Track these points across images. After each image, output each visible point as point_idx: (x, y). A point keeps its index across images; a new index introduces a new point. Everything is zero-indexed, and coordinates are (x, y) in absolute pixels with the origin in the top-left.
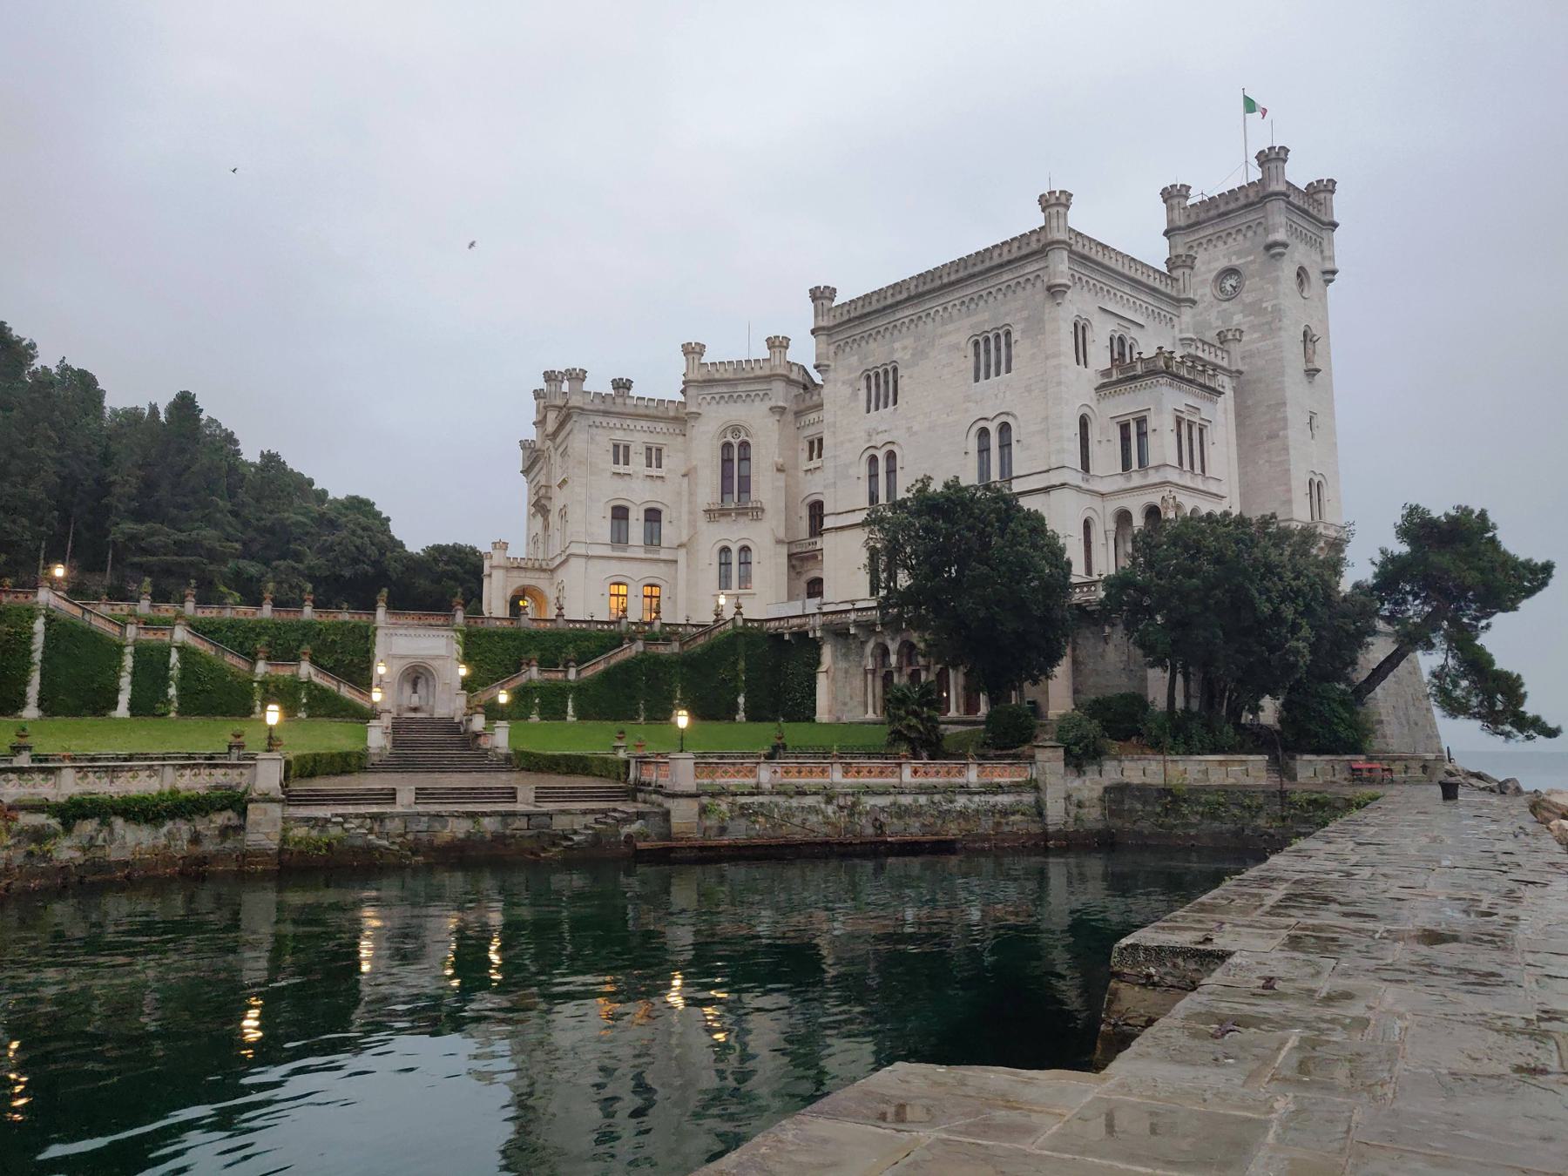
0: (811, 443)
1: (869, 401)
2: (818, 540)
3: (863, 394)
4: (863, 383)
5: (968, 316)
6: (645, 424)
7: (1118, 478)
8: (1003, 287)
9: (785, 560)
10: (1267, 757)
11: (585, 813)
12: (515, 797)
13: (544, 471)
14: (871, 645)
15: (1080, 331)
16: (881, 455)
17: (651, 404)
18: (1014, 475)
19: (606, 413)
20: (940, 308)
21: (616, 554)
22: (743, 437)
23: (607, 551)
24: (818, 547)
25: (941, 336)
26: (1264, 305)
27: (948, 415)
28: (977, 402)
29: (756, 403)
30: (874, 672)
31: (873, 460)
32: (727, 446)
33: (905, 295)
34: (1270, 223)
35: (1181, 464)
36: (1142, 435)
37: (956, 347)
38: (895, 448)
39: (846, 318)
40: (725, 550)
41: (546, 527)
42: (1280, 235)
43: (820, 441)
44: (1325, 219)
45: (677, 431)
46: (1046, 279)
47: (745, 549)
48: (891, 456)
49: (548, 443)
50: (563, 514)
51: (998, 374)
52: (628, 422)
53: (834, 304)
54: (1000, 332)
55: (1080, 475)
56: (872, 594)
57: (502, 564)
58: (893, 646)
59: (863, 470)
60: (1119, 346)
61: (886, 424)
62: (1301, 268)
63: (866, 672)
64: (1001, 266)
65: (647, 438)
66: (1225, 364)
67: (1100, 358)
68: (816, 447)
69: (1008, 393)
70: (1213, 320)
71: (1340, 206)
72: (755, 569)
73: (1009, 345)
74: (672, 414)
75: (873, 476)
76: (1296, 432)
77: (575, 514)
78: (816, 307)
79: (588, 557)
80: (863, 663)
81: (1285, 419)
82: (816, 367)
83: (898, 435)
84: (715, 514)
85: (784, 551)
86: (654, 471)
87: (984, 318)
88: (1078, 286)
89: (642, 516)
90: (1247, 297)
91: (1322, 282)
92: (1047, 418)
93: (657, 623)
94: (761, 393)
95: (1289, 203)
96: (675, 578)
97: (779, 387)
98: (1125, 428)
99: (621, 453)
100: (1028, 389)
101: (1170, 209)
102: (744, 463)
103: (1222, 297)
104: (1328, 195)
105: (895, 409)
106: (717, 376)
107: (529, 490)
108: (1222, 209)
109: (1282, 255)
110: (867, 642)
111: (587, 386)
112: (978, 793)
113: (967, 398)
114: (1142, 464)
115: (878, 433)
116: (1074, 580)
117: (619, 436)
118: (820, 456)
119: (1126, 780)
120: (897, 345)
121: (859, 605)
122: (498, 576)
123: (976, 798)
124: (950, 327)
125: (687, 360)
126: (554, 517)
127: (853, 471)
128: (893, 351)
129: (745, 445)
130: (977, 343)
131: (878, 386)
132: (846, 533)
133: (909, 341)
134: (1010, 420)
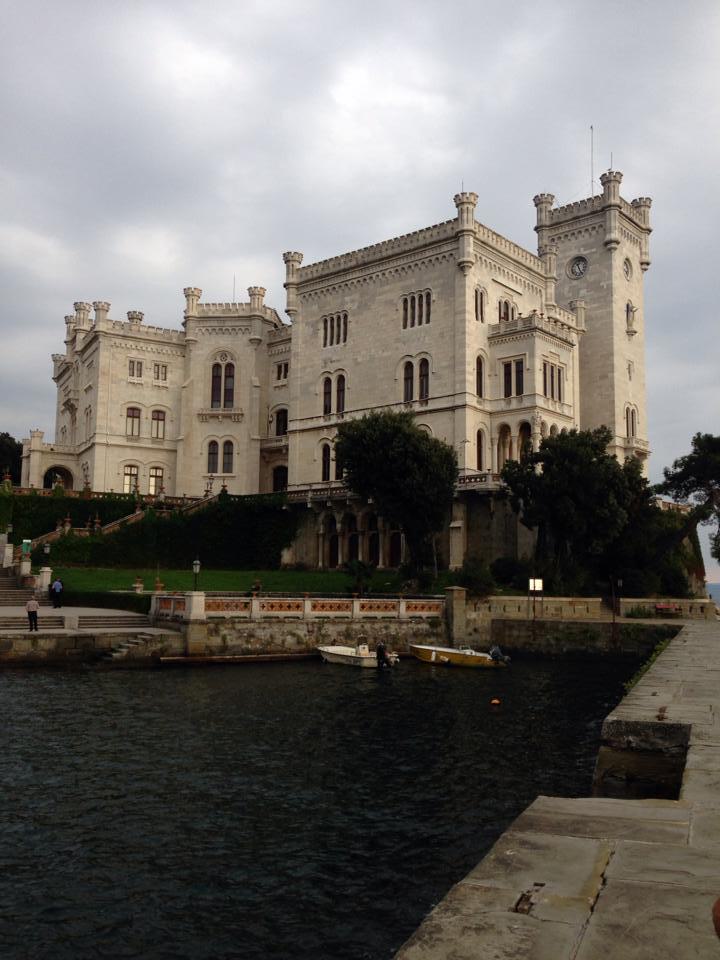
0: (280, 367)
1: (326, 339)
2: (283, 437)
3: (321, 333)
4: (322, 325)
5: (400, 281)
6: (153, 346)
7: (502, 402)
8: (426, 261)
9: (258, 452)
10: (600, 600)
11: (120, 635)
12: (63, 624)
13: (72, 378)
14: (321, 518)
15: (480, 297)
17: (159, 332)
19: (124, 337)
20: (379, 274)
21: (130, 444)
22: (229, 360)
23: (123, 441)
24: (283, 443)
26: (601, 284)
28: (404, 343)
29: (240, 335)
30: (324, 535)
31: (328, 382)
32: (217, 367)
33: (353, 263)
34: (608, 225)
35: (545, 394)
36: (520, 372)
37: (390, 303)
40: (213, 445)
41: (74, 420)
42: (616, 235)
43: (286, 365)
44: (643, 226)
45: (179, 353)
46: (457, 257)
47: (228, 444)
48: (341, 379)
49: (77, 357)
50: (89, 412)
51: (420, 323)
52: (142, 344)
53: (301, 266)
54: (423, 294)
55: (476, 399)
57: (39, 449)
58: (339, 517)
59: (320, 388)
60: (505, 310)
61: (341, 356)
62: (627, 259)
63: (318, 536)
64: (426, 246)
65: (155, 357)
66: (573, 324)
67: (492, 316)
68: (283, 370)
69: (427, 338)
70: (565, 293)
71: (655, 217)
72: (236, 460)
73: (428, 304)
74: (174, 341)
75: (327, 393)
76: (620, 374)
77: (100, 411)
78: (288, 267)
79: (107, 445)
80: (316, 528)
81: (613, 365)
82: (287, 311)
83: (347, 365)
84: (203, 417)
85: (258, 445)
86: (161, 383)
87: (412, 283)
88: (479, 263)
89: (150, 416)
90: (590, 278)
91: (640, 271)
92: (454, 357)
93: (162, 496)
94: (243, 328)
95: (621, 213)
96: (175, 463)
97: (257, 323)
98: (507, 367)
99: (135, 367)
100: (442, 335)
101: (540, 211)
102: (230, 380)
103: (574, 277)
104: (647, 209)
105: (345, 346)
106: (210, 314)
107: (59, 393)
108: (576, 214)
109: (615, 249)
110: (319, 514)
111: (110, 316)
112: (407, 623)
113: (398, 340)
114: (520, 391)
116: (468, 473)
117: (134, 354)
118: (285, 377)
119: (506, 614)
120: (347, 299)
121: (315, 487)
122: (35, 458)
123: (404, 627)
124: (387, 288)
125: (188, 300)
126: (80, 414)
127: (312, 388)
128: (343, 303)
129: (230, 367)
130: (406, 301)
131: (332, 327)
132: (305, 434)
133: (356, 296)
134: (428, 358)
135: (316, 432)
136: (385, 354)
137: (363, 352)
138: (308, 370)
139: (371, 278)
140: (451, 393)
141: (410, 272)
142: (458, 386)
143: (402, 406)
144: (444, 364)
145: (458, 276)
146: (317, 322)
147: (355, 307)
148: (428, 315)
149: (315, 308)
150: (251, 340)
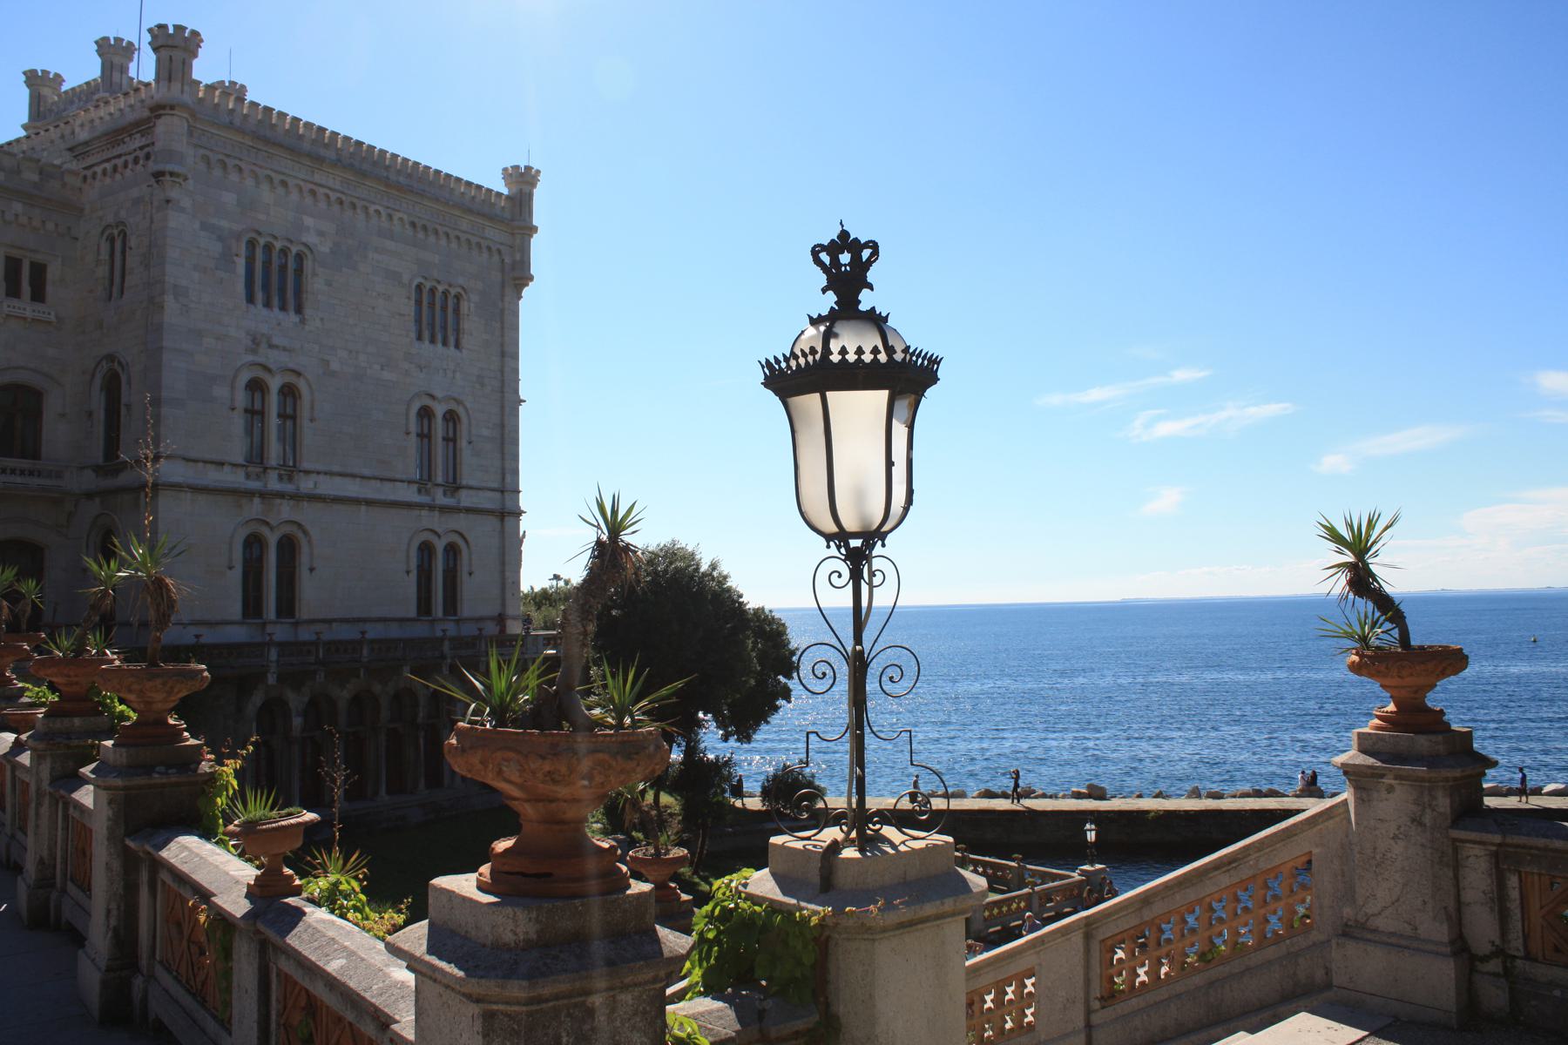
3: (241, 264)
16: (275, 384)
18: (464, 483)
27: (382, 369)
28: (421, 368)
31: (256, 386)
33: (330, 154)
38: (302, 385)
48: (288, 392)
56: (246, 614)
58: (296, 701)
69: (458, 375)
73: (457, 310)
92: (502, 426)
105: (303, 321)
115: (271, 346)
120: (309, 221)
127: (221, 392)
134: (461, 411)
136: (386, 375)
139: (366, 208)
140: (495, 485)
141: (432, 239)
142: (508, 479)
143: (415, 487)
144: (485, 432)
146: (238, 237)
147: (325, 248)
148: (457, 331)
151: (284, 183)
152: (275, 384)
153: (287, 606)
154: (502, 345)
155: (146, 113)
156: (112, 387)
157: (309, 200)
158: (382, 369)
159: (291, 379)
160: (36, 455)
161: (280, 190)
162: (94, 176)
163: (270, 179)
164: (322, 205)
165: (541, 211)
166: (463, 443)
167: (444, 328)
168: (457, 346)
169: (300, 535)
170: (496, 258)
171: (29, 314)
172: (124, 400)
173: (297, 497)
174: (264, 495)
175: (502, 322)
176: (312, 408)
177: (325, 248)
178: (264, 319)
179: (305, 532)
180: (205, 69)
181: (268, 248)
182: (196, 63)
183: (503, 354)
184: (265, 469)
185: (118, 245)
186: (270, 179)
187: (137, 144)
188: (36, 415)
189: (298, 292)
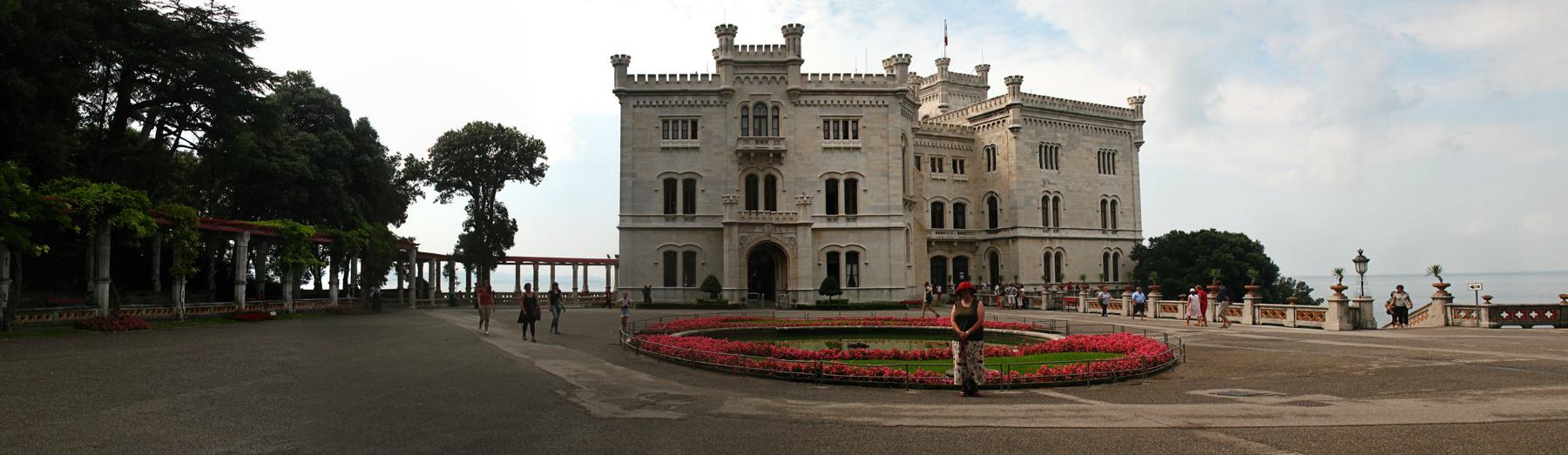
3: (1038, 154)
16: (1051, 197)
25: (1084, 141)
31: (1045, 199)
33: (1065, 109)
37: (1090, 150)
38: (1060, 196)
39: (1030, 105)
48: (1056, 200)
92: (1134, 204)
105: (1059, 173)
115: (1050, 184)
120: (1059, 135)
124: (1087, 138)
128: (1056, 137)
132: (1031, 241)
133: (1066, 135)
134: (1117, 200)
135: (1039, 241)
136: (1089, 189)
137: (1073, 183)
138: (1030, 185)
142: (1137, 225)
144: (1126, 207)
145: (1134, 149)
149: (1033, 132)
150: (913, 129)
151: (1050, 123)
152: (1051, 197)
153: (1059, 278)
154: (1132, 171)
155: (1004, 106)
156: (992, 202)
157: (1059, 127)
158: (1088, 186)
159: (1056, 194)
160: (964, 227)
161: (1049, 125)
162: (979, 128)
163: (1045, 122)
164: (1063, 128)
165: (1147, 108)
166: (1118, 213)
167: (1109, 168)
168: (1114, 173)
169: (1062, 251)
170: (1128, 136)
171: (961, 179)
172: (999, 207)
173: (1060, 238)
174: (1050, 238)
175: (1132, 162)
176: (1064, 205)
177: (1064, 144)
178: (1048, 173)
179: (1064, 250)
180: (1025, 88)
181: (1046, 147)
182: (1021, 86)
183: (1133, 175)
184: (1049, 229)
185: (991, 152)
186: (1045, 122)
187: (998, 117)
188: (963, 214)
189: (1056, 164)
